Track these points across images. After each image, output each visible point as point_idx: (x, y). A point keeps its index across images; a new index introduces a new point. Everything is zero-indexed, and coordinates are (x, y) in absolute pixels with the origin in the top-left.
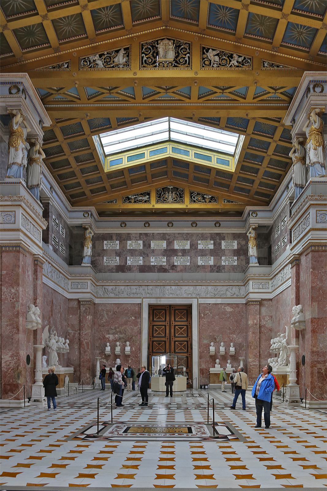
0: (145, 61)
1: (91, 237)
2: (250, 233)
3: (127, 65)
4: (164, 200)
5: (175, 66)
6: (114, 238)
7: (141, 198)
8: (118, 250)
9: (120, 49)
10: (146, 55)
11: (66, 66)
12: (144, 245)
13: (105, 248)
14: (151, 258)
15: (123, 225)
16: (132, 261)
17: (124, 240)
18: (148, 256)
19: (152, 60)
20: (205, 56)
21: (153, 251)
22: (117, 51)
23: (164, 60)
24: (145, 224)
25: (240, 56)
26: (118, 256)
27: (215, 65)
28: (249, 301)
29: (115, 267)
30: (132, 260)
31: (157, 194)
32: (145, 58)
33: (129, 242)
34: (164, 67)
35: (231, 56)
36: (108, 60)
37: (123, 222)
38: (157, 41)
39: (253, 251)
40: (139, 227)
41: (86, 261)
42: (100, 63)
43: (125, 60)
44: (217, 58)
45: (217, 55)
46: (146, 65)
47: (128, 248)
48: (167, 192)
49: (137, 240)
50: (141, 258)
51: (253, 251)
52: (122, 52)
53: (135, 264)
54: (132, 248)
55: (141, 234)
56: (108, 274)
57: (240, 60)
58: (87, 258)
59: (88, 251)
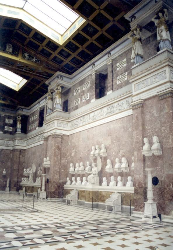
2: (19, 117)
5: (12, 54)
20: (23, 54)
23: (8, 51)
25: (36, 59)
27: (27, 59)
28: (15, 150)
35: (33, 58)
39: (19, 126)
44: (28, 57)
45: (28, 56)
51: (19, 126)
57: (36, 60)
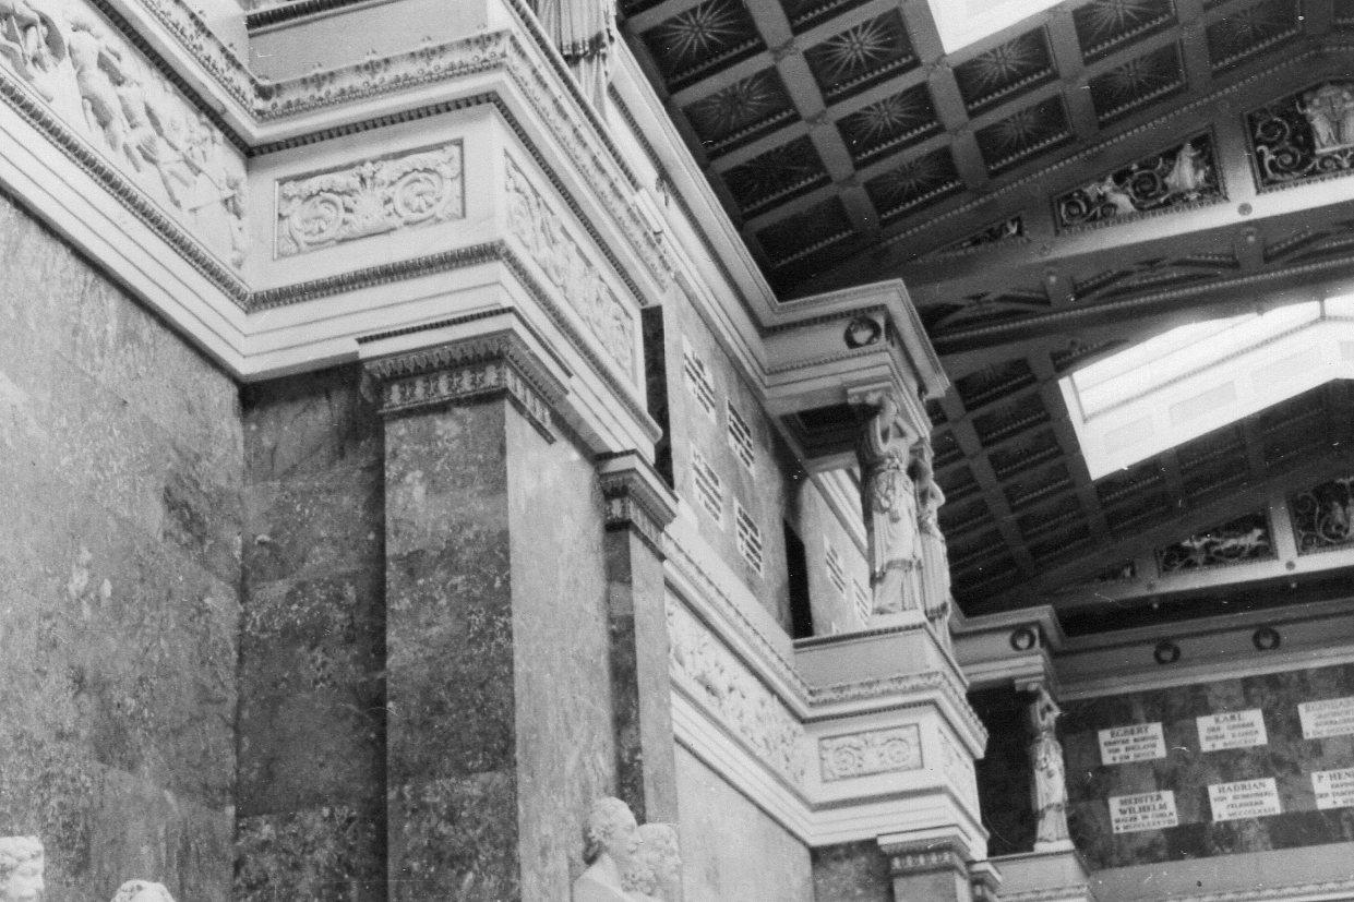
0: (1272, 164)
1: (1053, 723)
3: (1213, 190)
4: (1332, 536)
6: (1140, 713)
7: (1231, 543)
8: (1162, 761)
9: (1180, 148)
10: (1270, 145)
11: (1014, 230)
12: (1272, 726)
13: (1107, 759)
14: (1315, 776)
15: (1167, 655)
16: (1230, 800)
17: (1182, 716)
18: (1296, 771)
19: (1294, 156)
21: (1317, 747)
22: (1172, 155)
23: (1337, 148)
24: (1256, 638)
26: (1167, 788)
29: (1162, 837)
30: (1230, 796)
31: (1297, 515)
32: (1269, 157)
33: (1204, 723)
34: (1340, 168)
36: (1146, 187)
37: (1164, 644)
38: (1300, 96)
40: (1232, 656)
41: (1053, 833)
42: (1123, 201)
43: (1201, 175)
46: (1279, 177)
47: (1206, 747)
48: (1336, 504)
49: (1236, 709)
50: (1270, 783)
52: (1187, 155)
53: (1245, 813)
54: (1219, 746)
55: (1247, 683)
56: (1138, 869)
58: (1051, 814)
59: (1051, 784)
